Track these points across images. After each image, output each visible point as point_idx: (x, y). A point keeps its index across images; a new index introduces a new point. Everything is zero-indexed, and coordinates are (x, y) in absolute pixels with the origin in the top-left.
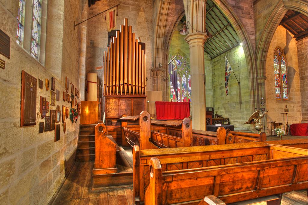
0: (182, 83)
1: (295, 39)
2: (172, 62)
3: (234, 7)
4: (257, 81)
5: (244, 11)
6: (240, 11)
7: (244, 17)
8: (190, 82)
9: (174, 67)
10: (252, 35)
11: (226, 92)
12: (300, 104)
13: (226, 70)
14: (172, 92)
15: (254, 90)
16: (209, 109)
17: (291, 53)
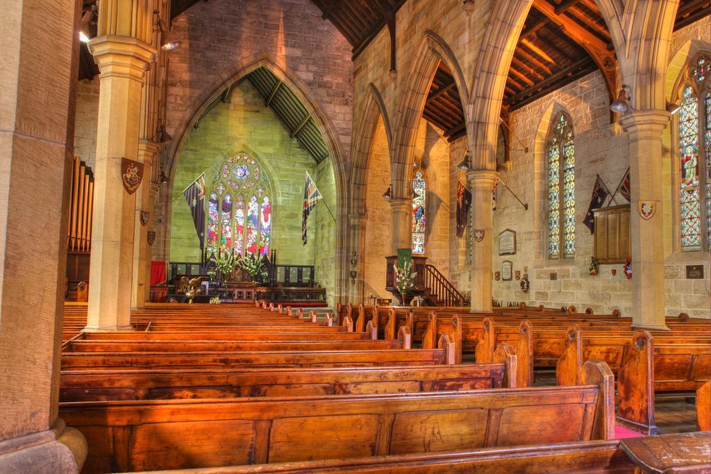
0: (249, 214)
1: (446, 139)
2: (196, 183)
3: (309, 84)
5: (333, 90)
6: (323, 92)
7: (331, 103)
8: (266, 213)
9: (200, 192)
10: (346, 134)
11: (303, 239)
12: (447, 264)
13: (306, 197)
14: (226, 233)
15: (342, 236)
16: (304, 269)
17: (434, 167)
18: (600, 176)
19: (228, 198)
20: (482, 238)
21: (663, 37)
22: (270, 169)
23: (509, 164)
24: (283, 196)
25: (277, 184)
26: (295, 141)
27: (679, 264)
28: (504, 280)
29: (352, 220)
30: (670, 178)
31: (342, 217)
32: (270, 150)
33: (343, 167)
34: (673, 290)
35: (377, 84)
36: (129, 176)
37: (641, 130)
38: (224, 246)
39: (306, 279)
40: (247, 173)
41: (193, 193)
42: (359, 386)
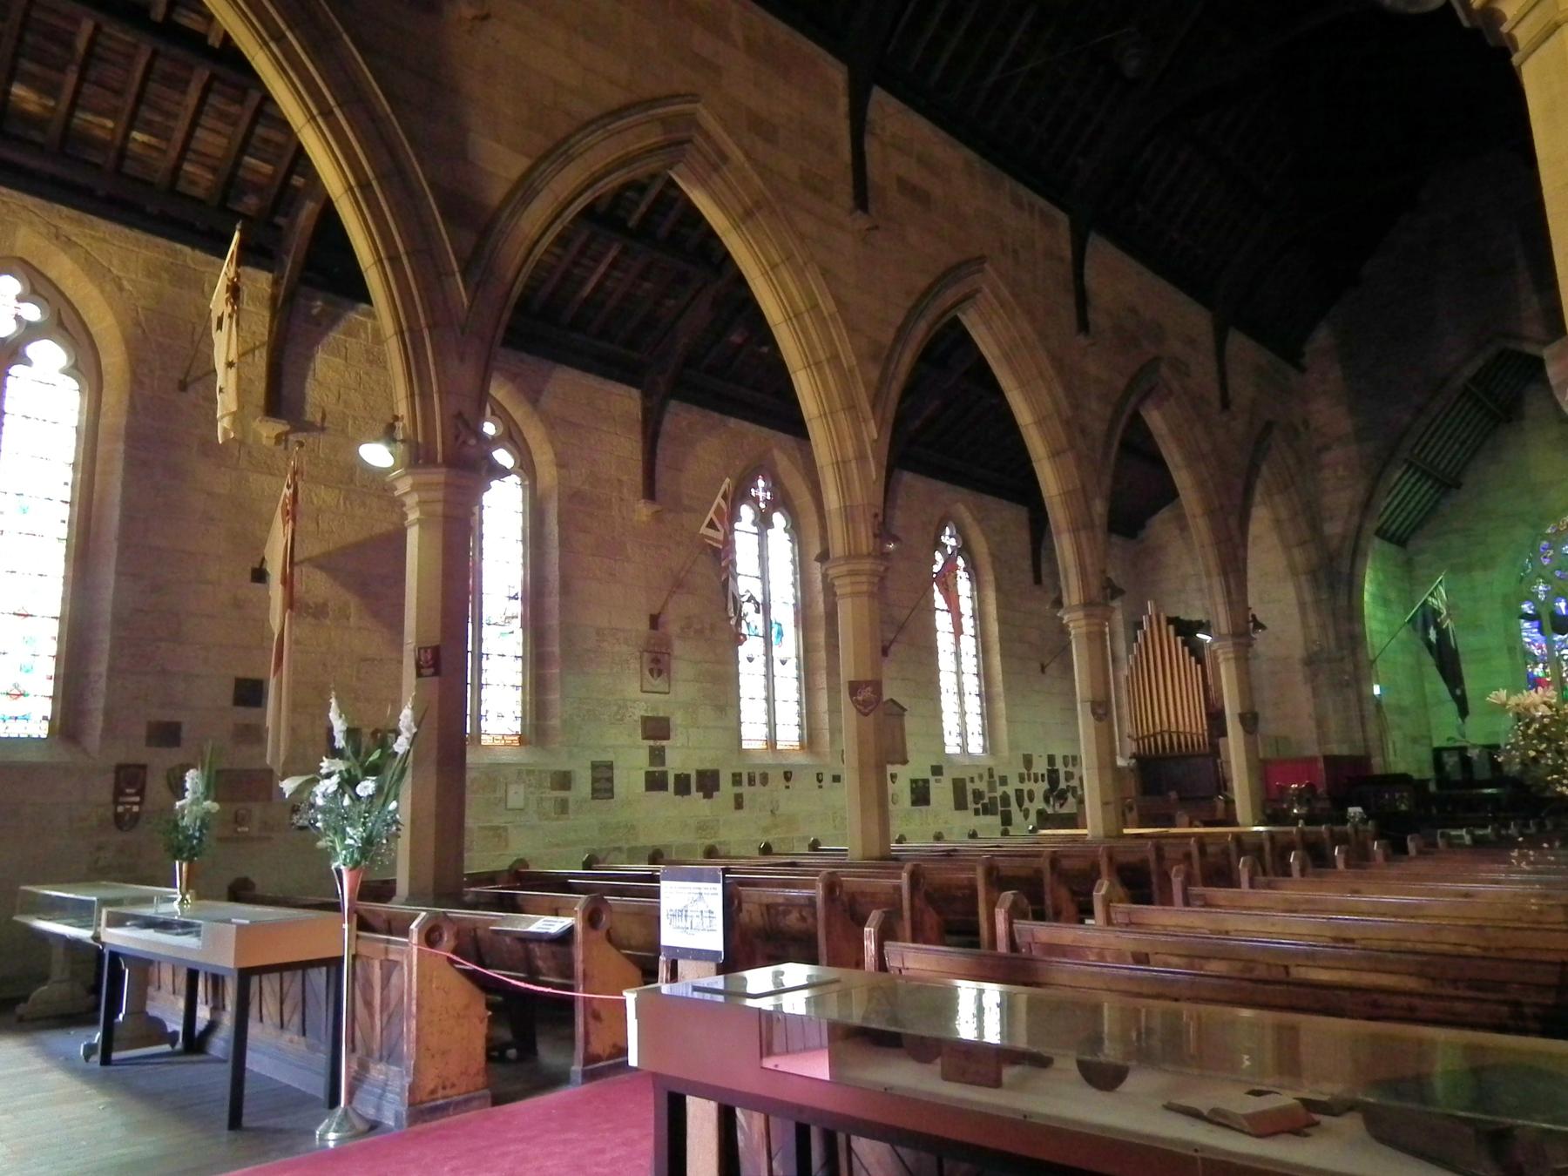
19: (1562, 605)
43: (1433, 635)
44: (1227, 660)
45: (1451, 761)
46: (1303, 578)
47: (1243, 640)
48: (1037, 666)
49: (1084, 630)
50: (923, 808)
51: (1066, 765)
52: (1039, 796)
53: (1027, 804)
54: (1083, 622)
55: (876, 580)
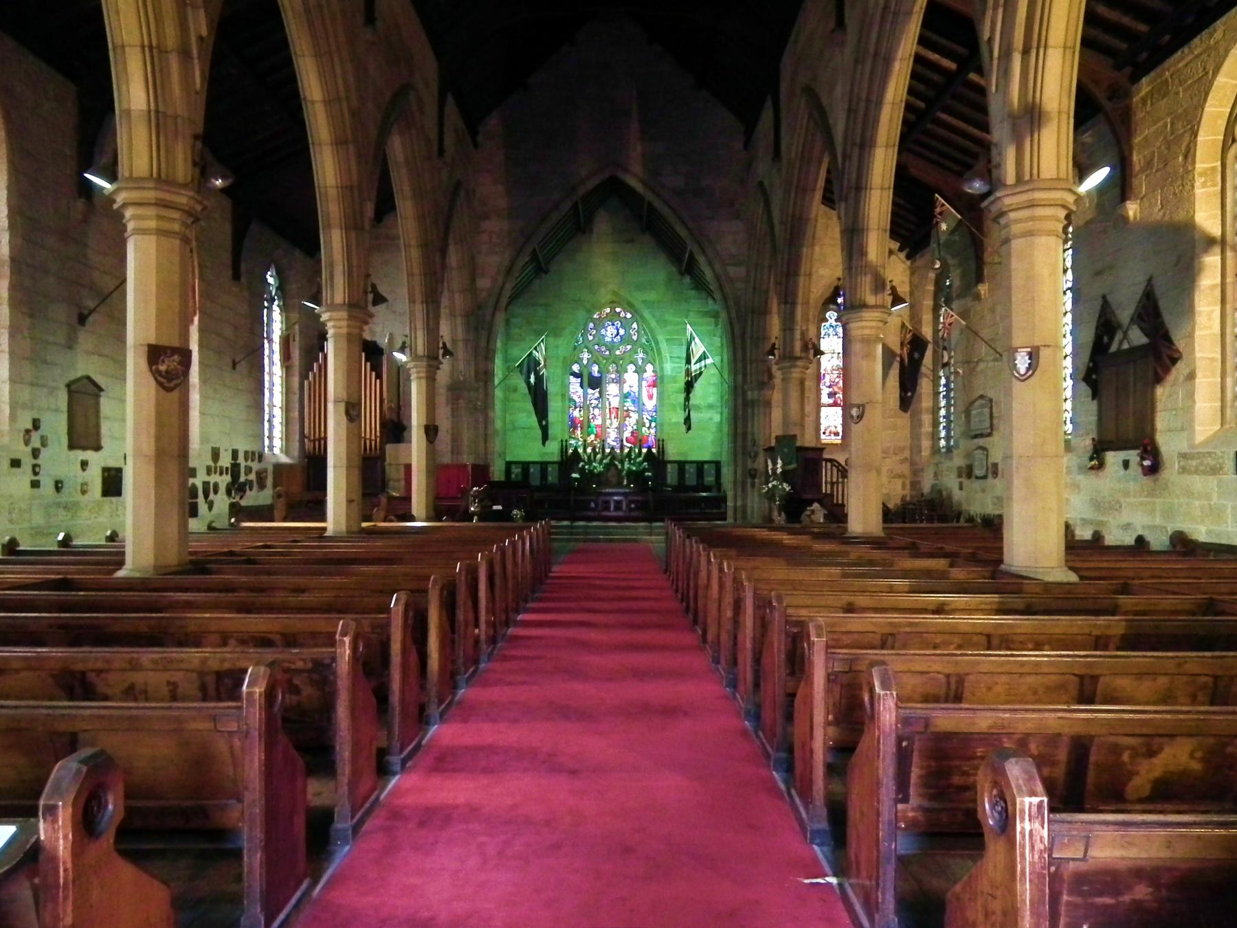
1: (902, 255)
4: (744, 393)
13: (688, 361)
16: (706, 466)
18: (1109, 298)
20: (860, 417)
21: (1051, 42)
22: (653, 324)
23: (983, 289)
24: (673, 362)
25: (663, 345)
26: (687, 279)
27: (1224, 449)
28: (977, 478)
29: (749, 393)
30: (1218, 292)
31: (735, 388)
32: (652, 296)
33: (734, 314)
34: (1215, 496)
35: (766, 183)
36: (163, 368)
37: (1016, 221)
38: (593, 437)
39: (709, 479)
40: (622, 332)
41: (531, 365)
42: (103, 676)
43: (532, 380)
44: (419, 378)
45: (516, 470)
46: (459, 321)
47: (433, 363)
48: (228, 360)
49: (345, 331)
50: (114, 499)
51: (246, 460)
52: (222, 489)
53: (212, 496)
54: (344, 323)
55: (190, 221)
